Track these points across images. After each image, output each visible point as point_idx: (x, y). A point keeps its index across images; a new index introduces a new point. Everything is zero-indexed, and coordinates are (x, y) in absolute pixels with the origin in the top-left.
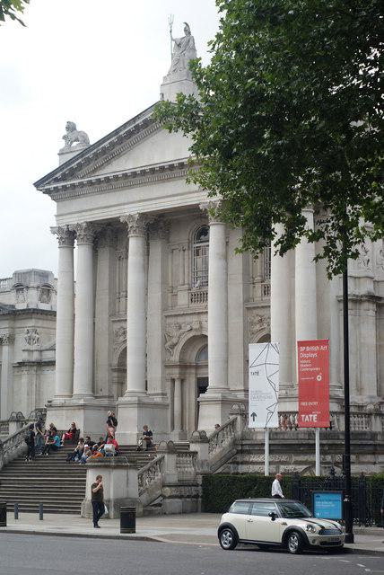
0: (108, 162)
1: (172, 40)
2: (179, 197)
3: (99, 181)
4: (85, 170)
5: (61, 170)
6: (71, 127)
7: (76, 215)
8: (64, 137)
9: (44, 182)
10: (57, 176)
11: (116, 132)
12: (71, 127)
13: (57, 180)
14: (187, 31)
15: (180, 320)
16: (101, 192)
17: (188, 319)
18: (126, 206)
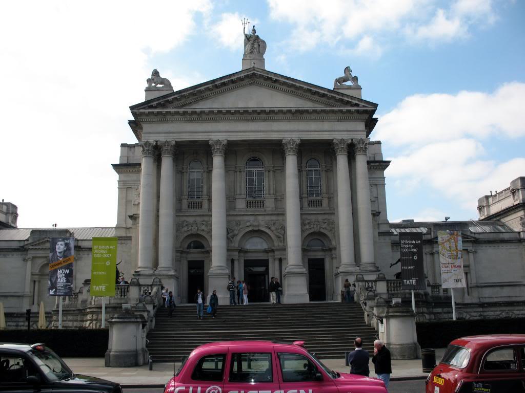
0: (196, 101)
1: (245, 34)
2: (262, 133)
3: (194, 113)
4: (176, 103)
5: (158, 100)
6: (156, 73)
7: (163, 135)
8: (148, 81)
9: (138, 107)
10: (152, 104)
11: (213, 81)
12: (156, 73)
13: (151, 107)
14: (254, 31)
15: (239, 218)
16: (191, 121)
17: (246, 218)
18: (212, 134)
